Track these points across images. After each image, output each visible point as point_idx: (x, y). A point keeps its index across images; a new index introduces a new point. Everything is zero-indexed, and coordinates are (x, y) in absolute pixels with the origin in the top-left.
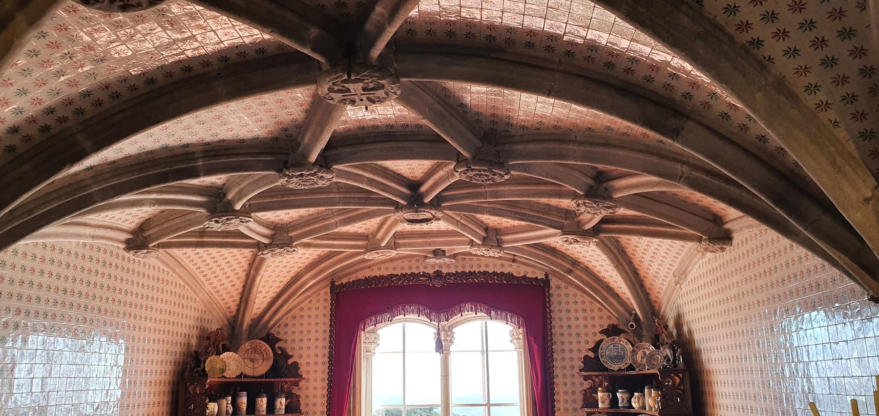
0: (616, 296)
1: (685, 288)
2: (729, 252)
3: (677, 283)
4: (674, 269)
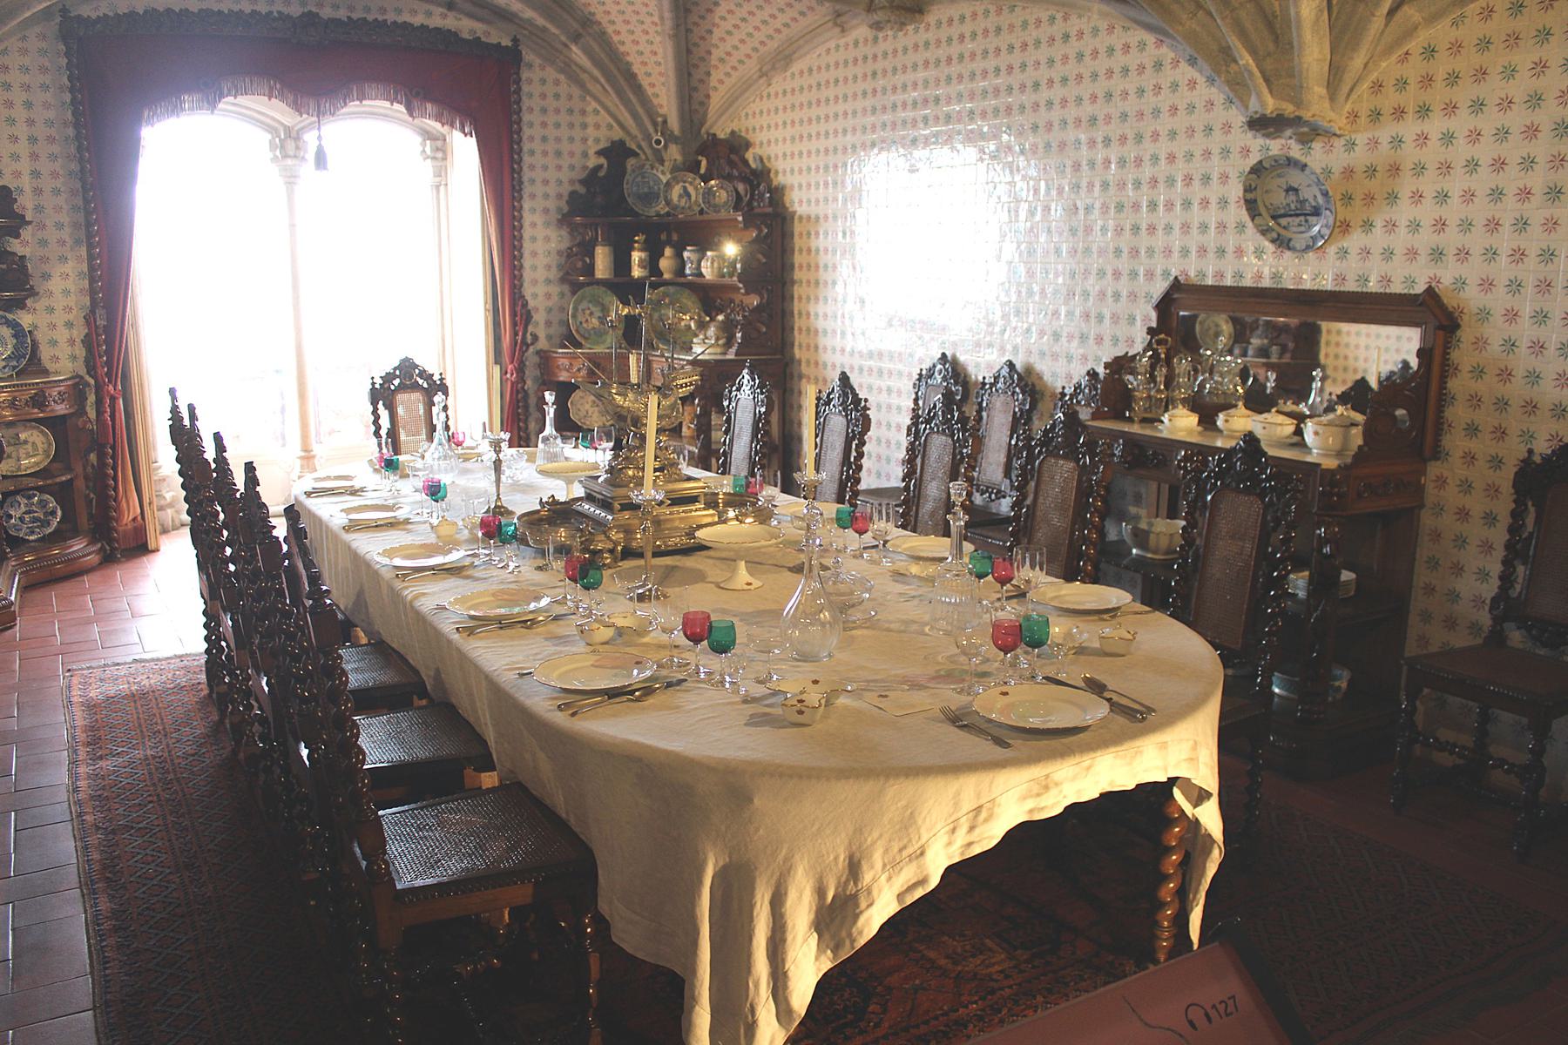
0: (638, 89)
1: (778, 83)
2: (911, 35)
3: (763, 74)
4: (762, 49)
